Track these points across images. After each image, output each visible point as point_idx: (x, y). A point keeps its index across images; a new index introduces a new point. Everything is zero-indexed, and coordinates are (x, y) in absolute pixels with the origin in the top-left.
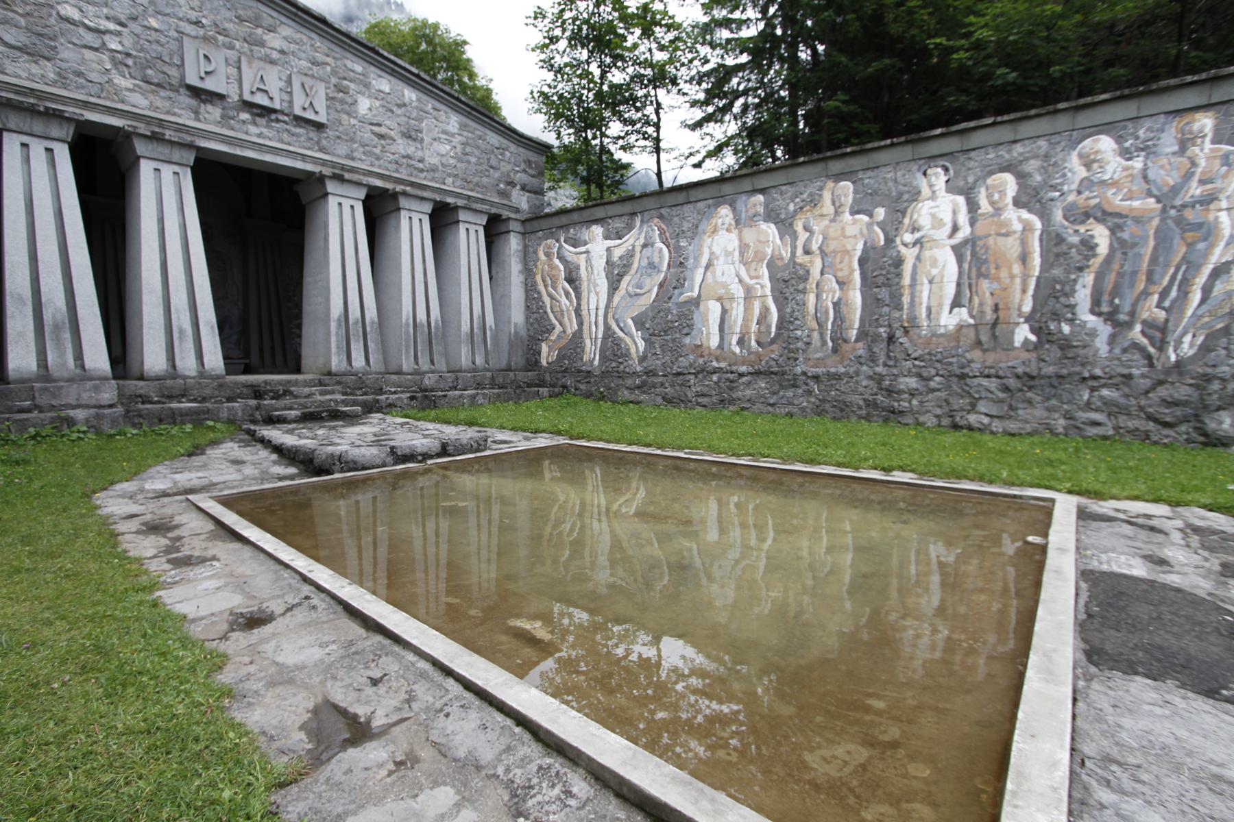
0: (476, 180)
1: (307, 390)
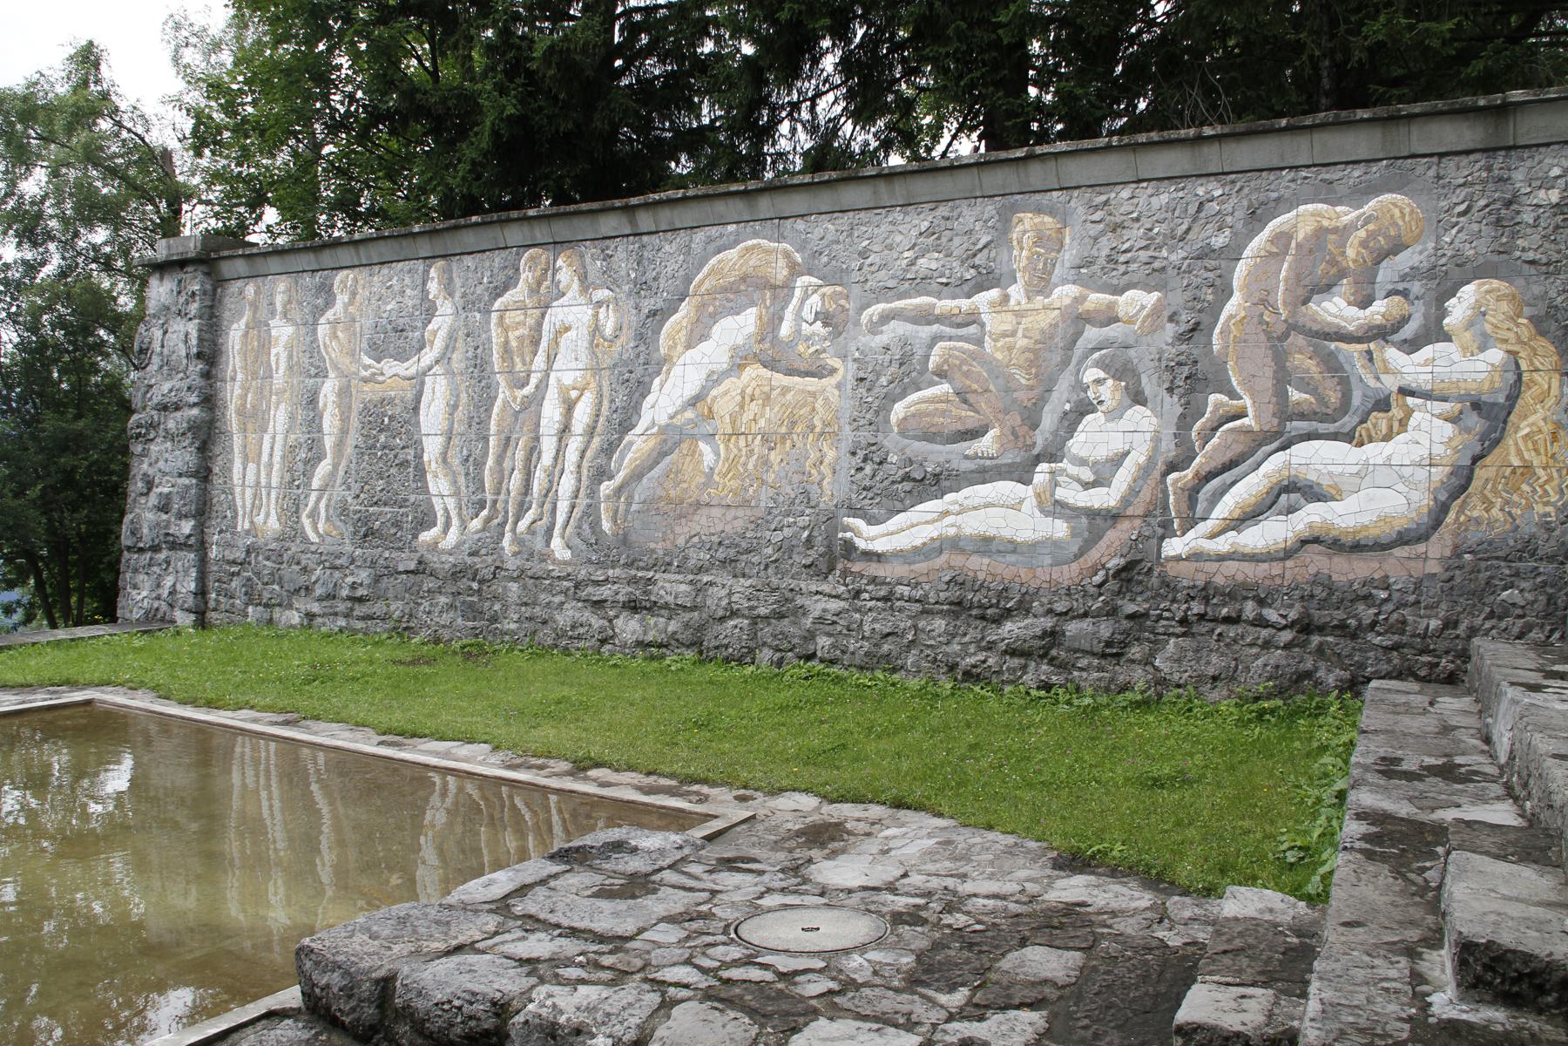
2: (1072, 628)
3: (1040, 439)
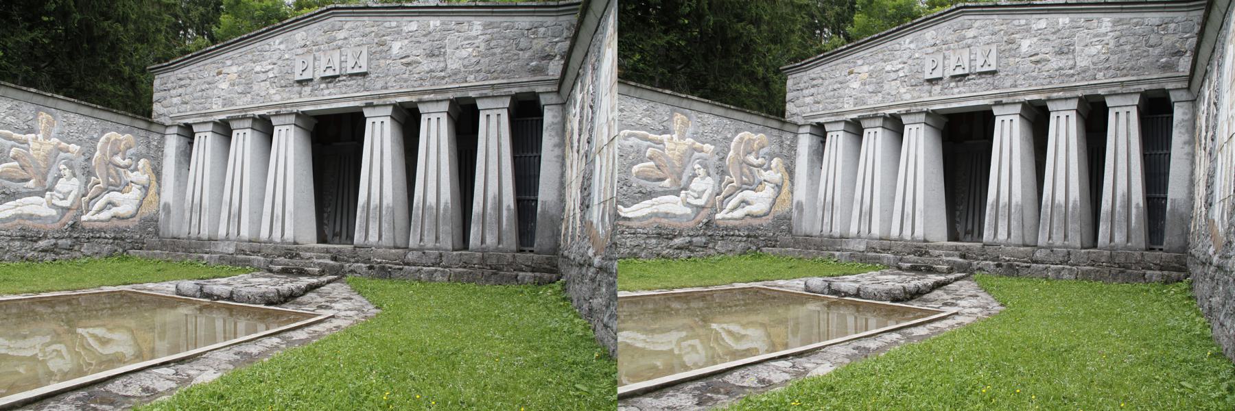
0: (1129, 65)
1: (937, 252)
2: (695, 239)
3: (683, 183)
